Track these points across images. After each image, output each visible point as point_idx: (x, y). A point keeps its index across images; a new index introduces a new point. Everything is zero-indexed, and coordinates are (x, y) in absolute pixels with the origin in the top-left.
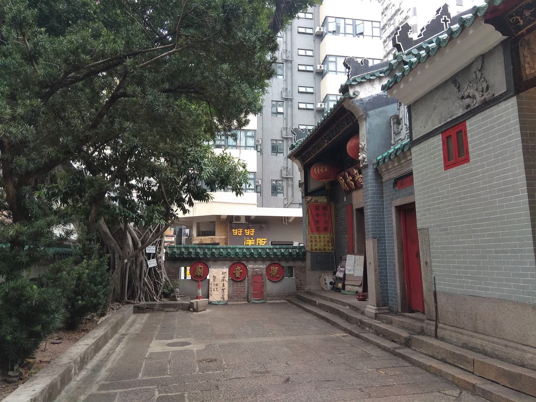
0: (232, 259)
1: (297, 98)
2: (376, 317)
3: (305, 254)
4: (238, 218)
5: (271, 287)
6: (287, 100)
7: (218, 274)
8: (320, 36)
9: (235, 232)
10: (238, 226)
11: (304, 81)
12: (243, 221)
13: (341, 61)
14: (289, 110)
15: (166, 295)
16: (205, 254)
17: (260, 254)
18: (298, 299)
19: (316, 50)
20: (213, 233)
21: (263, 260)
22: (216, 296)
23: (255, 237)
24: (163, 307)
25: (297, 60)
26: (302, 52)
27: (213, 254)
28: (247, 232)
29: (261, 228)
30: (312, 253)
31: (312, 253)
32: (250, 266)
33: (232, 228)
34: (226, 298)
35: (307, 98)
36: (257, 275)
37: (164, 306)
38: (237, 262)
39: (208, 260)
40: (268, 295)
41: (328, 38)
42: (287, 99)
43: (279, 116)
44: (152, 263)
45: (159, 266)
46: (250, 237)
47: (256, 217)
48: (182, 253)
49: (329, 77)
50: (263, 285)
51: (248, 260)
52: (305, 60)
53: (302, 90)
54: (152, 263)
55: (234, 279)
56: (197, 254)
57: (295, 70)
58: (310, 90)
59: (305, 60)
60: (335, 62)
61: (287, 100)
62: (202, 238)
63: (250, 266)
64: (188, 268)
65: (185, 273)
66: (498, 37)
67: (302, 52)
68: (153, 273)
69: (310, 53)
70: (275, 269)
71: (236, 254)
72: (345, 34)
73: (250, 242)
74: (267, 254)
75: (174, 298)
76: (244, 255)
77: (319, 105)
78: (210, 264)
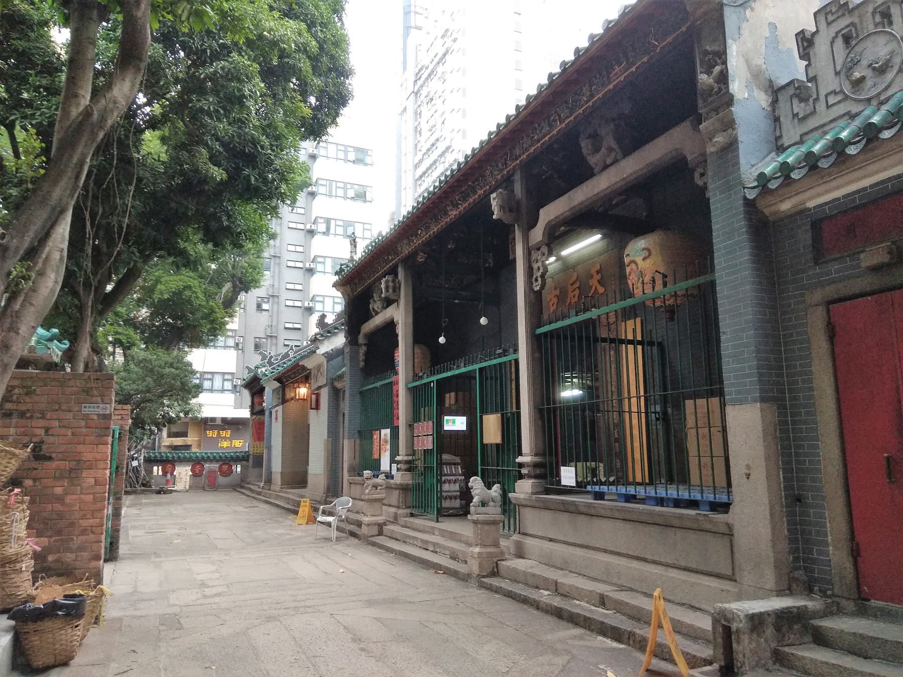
0: (193, 461)
1: (284, 295)
2: (263, 488)
3: (248, 456)
4: (213, 419)
5: (221, 480)
6: (273, 297)
7: (183, 473)
8: (311, 232)
9: (210, 433)
10: (213, 427)
11: (292, 277)
12: (219, 422)
13: (329, 262)
14: (275, 307)
15: (144, 485)
16: (173, 457)
17: (215, 457)
18: (239, 486)
19: (307, 246)
20: (184, 434)
21: (217, 461)
22: (179, 486)
23: (230, 439)
24: (143, 492)
25: (286, 256)
26: (291, 248)
27: (179, 457)
28: (223, 434)
29: (238, 429)
30: (254, 456)
31: (254, 456)
32: (206, 466)
33: (206, 429)
34: (187, 487)
35: (295, 295)
36: (211, 472)
37: (144, 491)
38: (197, 463)
39: (175, 461)
40: (219, 486)
41: (317, 238)
42: (273, 296)
43: (264, 313)
44: (135, 463)
45: (139, 465)
46: (225, 439)
47: (233, 418)
48: (156, 456)
49: (316, 278)
50: (215, 479)
51: (206, 461)
52: (294, 256)
53: (290, 286)
54: (135, 463)
55: (195, 475)
56: (167, 457)
57: (283, 267)
58: (299, 287)
59: (294, 256)
60: (324, 263)
61: (273, 297)
62: (173, 439)
63: (206, 466)
64: (160, 468)
65: (157, 470)
66: (279, 384)
67: (291, 248)
68: (136, 470)
69: (300, 249)
70: (225, 467)
71: (197, 457)
72: (336, 235)
73: (225, 444)
74: (220, 457)
75: (150, 486)
76: (203, 457)
77: (306, 304)
78: (176, 464)
